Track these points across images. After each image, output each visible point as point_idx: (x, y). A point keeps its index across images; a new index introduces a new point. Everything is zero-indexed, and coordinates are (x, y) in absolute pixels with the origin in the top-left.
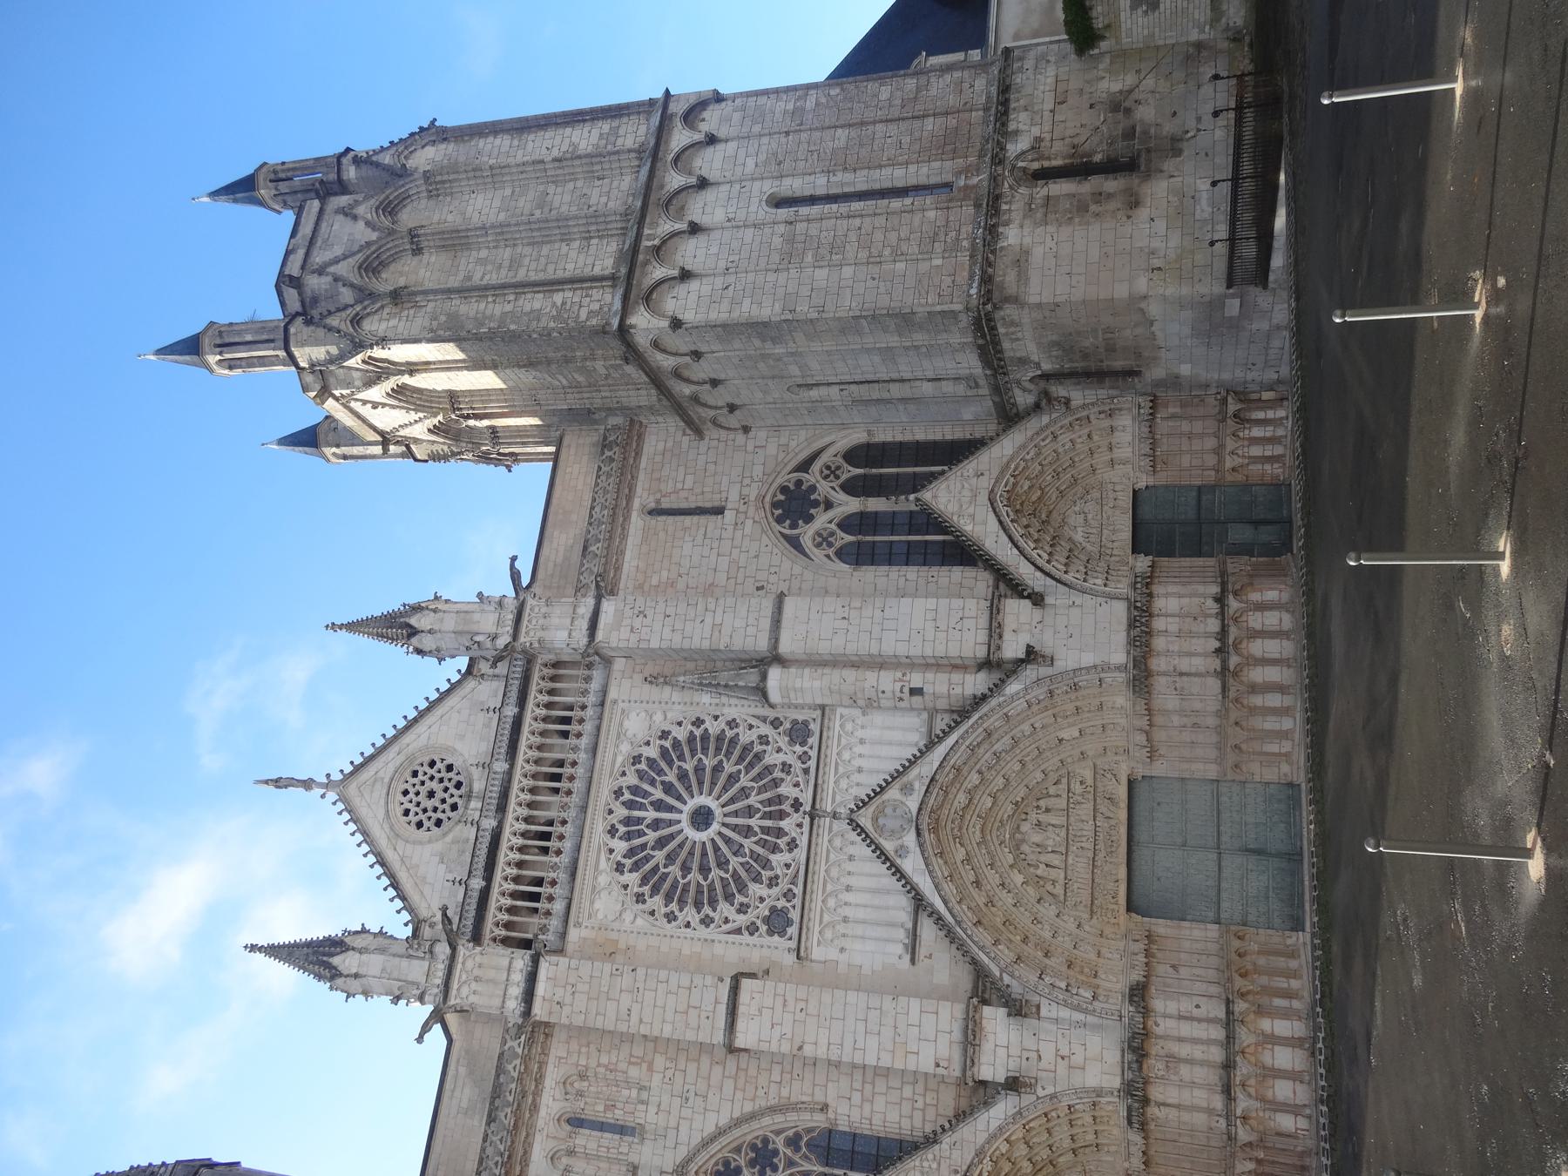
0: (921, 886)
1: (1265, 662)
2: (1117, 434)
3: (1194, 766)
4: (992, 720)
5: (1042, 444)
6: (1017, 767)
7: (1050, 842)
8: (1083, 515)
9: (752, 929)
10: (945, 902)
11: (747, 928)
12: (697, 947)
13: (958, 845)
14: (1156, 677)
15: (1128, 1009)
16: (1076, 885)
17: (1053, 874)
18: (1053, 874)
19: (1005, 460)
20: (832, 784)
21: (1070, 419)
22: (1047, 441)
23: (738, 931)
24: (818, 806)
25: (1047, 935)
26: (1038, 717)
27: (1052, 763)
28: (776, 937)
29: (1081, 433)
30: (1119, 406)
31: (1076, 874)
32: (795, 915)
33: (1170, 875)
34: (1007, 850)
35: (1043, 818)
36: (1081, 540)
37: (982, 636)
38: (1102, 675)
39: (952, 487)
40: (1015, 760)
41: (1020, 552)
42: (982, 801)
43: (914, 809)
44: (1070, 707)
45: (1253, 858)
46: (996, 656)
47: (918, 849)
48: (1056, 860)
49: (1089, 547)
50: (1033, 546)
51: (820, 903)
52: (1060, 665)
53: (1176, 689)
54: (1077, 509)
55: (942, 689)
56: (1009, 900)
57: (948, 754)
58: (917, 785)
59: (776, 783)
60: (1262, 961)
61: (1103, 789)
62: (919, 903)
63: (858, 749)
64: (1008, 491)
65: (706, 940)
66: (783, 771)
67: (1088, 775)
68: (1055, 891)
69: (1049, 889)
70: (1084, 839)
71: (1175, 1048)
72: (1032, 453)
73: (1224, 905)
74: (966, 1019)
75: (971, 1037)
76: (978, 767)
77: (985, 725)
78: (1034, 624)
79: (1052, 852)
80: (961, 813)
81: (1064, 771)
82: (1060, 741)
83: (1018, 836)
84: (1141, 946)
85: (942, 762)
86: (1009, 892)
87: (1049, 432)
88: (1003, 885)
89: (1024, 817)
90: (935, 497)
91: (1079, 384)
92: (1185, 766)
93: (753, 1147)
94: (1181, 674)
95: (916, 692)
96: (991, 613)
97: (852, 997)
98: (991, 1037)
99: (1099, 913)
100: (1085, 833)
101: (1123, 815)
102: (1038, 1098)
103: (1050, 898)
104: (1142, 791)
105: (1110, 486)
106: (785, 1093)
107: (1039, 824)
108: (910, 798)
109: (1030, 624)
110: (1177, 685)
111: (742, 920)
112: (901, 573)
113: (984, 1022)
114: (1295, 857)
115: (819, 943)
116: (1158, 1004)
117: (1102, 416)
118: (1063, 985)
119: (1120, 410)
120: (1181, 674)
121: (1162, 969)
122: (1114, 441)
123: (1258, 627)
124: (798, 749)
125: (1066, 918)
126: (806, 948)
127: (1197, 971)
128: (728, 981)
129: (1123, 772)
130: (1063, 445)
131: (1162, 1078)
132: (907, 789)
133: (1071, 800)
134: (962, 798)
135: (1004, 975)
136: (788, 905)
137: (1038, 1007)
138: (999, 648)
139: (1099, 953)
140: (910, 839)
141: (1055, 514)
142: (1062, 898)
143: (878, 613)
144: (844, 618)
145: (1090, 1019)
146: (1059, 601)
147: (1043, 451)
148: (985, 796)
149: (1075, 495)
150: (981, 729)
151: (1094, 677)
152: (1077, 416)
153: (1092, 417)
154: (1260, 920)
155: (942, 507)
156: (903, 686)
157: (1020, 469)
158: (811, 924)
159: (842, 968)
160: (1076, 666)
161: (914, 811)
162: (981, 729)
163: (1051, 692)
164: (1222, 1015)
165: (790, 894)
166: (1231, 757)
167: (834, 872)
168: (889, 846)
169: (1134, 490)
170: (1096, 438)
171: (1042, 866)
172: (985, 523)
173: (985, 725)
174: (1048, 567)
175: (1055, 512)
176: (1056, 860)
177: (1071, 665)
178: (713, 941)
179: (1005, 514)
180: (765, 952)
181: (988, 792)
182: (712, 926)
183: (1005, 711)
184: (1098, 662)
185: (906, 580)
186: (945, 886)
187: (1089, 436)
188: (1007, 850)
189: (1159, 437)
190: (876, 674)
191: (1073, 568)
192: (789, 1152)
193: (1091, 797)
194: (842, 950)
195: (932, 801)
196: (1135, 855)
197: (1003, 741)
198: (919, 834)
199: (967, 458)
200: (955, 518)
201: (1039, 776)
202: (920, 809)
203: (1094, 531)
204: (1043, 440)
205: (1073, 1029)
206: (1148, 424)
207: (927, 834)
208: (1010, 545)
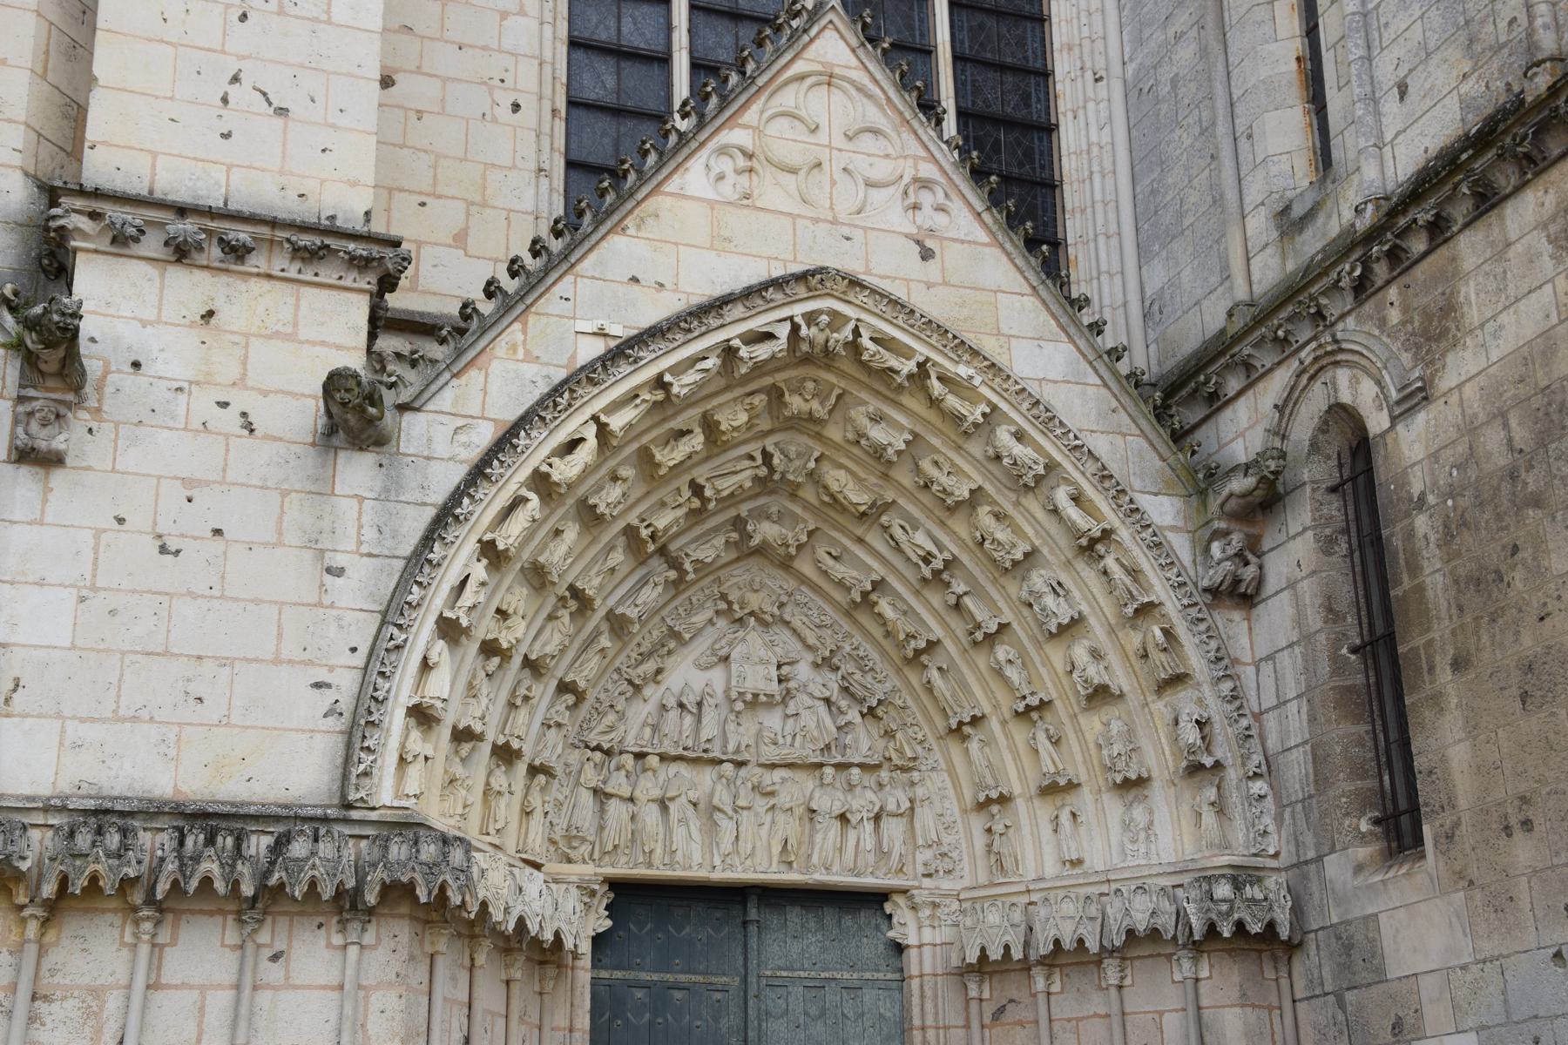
2: (1114, 807)
5: (1062, 496)
8: (774, 688)
21: (1172, 606)
22: (1072, 512)
29: (1113, 658)
30: (1234, 798)
39: (867, 142)
41: (589, 367)
46: (83, 223)
49: (641, 711)
50: (616, 422)
54: (803, 671)
64: (854, 346)
72: (1018, 450)
78: (240, 401)
87: (1112, 519)
90: (829, 79)
91: (1331, 612)
96: (304, 228)
105: (896, 798)
109: (240, 383)
117: (1191, 735)
119: (1220, 808)
122: (1085, 799)
130: (1057, 589)
138: (122, 240)
141: (779, 582)
146: (348, 508)
147: (1033, 504)
149: (861, 663)
152: (1181, 630)
153: (1185, 702)
155: (788, 98)
157: (952, 401)
169: (874, 900)
170: (1093, 724)
172: (720, 242)
174: (514, 478)
175: (791, 584)
179: (756, 324)
185: (504, 15)
187: (1100, 695)
189: (1112, 977)
191: (517, 597)
199: (995, 200)
203: (710, 728)
206: (1166, 922)
208: (619, 330)
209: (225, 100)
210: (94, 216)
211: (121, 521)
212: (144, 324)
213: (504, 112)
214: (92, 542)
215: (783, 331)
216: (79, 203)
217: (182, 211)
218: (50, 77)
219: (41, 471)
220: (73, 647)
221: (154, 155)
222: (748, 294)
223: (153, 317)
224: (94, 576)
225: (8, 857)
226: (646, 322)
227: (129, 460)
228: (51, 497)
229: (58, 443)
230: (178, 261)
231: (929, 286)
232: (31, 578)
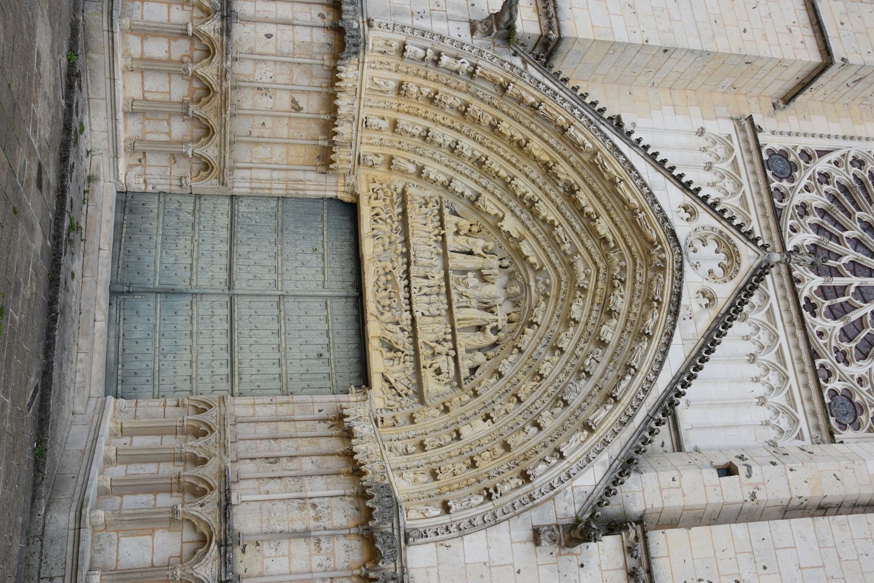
0: (651, 169)
3: (269, 411)
4: (612, 418)
6: (545, 369)
7: (472, 279)
9: (807, 156)
10: (614, 145)
11: (810, 158)
12: (859, 131)
13: (610, 238)
14: (353, 523)
16: (430, 227)
17: (462, 242)
18: (462, 242)
20: (781, 332)
23: (822, 153)
25: (467, 145)
26: (533, 442)
27: (489, 388)
28: (777, 147)
31: (431, 242)
33: (300, 257)
34: (532, 259)
35: (488, 316)
38: (446, 519)
40: (550, 379)
42: (586, 311)
43: (689, 273)
44: (484, 465)
45: (182, 286)
46: (632, 535)
47: (669, 216)
48: (458, 261)
51: (744, 181)
52: (521, 529)
53: (314, 506)
55: (689, 477)
56: (523, 185)
57: (665, 353)
58: (696, 308)
59: (846, 335)
61: (408, 364)
65: (852, 138)
66: (844, 353)
67: (431, 384)
68: (455, 219)
69: (464, 220)
70: (426, 290)
73: (224, 221)
76: (609, 351)
77: (620, 408)
79: (465, 272)
80: (616, 282)
81: (467, 386)
82: (487, 417)
83: (517, 289)
84: (344, 129)
85: (670, 340)
86: (522, 196)
88: (532, 202)
89: (514, 316)
92: (283, 410)
94: (305, 534)
95: (728, 470)
99: (395, 193)
100: (426, 299)
101: (373, 328)
103: (459, 207)
104: (345, 367)
107: (489, 309)
108: (699, 288)
110: (312, 513)
111: (822, 165)
113: (535, 17)
114: (119, 288)
115: (729, 137)
116: (322, 37)
118: (445, 59)
120: (305, 534)
121: (312, 104)
124: (835, 384)
125: (442, 178)
126: (743, 130)
127: (264, 102)
128: (837, 59)
133: (450, 345)
134: (620, 303)
137: (473, 31)
138: (630, 550)
139: (395, 125)
140: (683, 230)
142: (446, 211)
145: (407, 21)
148: (583, 320)
150: (625, 401)
151: (459, 515)
154: (176, 205)
158: (746, 157)
159: (696, 111)
161: (687, 267)
162: (625, 401)
163: (526, 477)
166: (210, 417)
168: (705, 219)
171: (478, 250)
173: (620, 408)
176: (458, 261)
178: (844, 138)
180: (785, 128)
181: (581, 326)
182: (850, 159)
183: (594, 437)
184: (456, 544)
190: (795, 493)
193: (424, 352)
194: (701, 132)
195: (668, 283)
196: (350, 279)
197: (581, 397)
198: (673, 233)
201: (506, 368)
202: (681, 269)
205: (427, 10)
207: (663, 237)
209: (700, 580)
210: (636, 538)
211: (519, 572)
212: (599, 566)
214: (508, 563)
216: (640, 532)
217: (649, 571)
218: (685, 512)
219: (532, 539)
220: (466, 564)
221: (668, 556)
223: (603, 568)
224: (495, 566)
225: (383, 558)
227: (544, 571)
228: (523, 544)
229: (544, 543)
230: (629, 574)
232: (490, 543)
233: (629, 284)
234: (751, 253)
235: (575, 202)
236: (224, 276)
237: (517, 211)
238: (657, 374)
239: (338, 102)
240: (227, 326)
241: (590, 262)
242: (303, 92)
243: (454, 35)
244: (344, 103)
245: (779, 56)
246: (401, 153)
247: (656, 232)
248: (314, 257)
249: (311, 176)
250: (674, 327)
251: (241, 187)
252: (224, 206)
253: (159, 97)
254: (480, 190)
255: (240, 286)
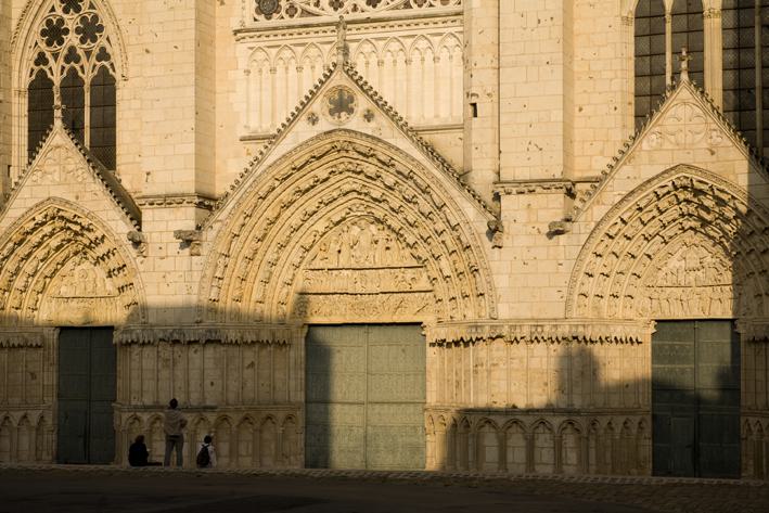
1: (503, 449)
4: (438, 192)
13: (330, 170)
15: (201, 329)
16: (324, 279)
19: (732, 177)
24: (349, 26)
32: (275, 21)
36: (671, 266)
37: (523, 174)
58: (373, 124)
60: (267, 435)
62: (273, 139)
63: (429, 56)
67: (424, 284)
71: (181, 366)
74: (183, 195)
75: (168, 201)
80: (358, 170)
84: (265, 336)
85: (393, 147)
93: (96, 17)
97: (190, 92)
98: (172, 217)
102: (135, 259)
106: (133, 40)
109: (537, 221)
110: (479, 368)
112: (619, 73)
116: (210, 351)
118: (218, 274)
123: (538, 443)
126: (244, 38)
127: (250, 384)
129: (428, 318)
131: (158, 357)
132: (369, 117)
135: (219, 224)
136: (283, 13)
143: (545, 58)
144: (539, 21)
150: (428, 182)
156: (477, 95)
160: (494, 270)
164: (208, 403)
165: (293, 11)
167: (287, 54)
172: (652, 162)
174: (600, 235)
177: (494, 266)
179: (662, 184)
185: (611, 80)
186: (287, 163)
188: (343, 215)
192: (96, 51)
194: (248, 72)
195: (358, 141)
196: (355, 330)
200: (657, 129)
203: (681, 277)
204: (759, 219)
208: (624, 193)
213: (612, 111)
215: (670, 184)
222: (657, 176)
226: (631, 189)
231: (713, 163)
233: (358, 162)
234: (338, 77)
235: (307, 190)
236: (355, 407)
237: (311, 223)
238: (413, 160)
239: (249, 341)
240: (386, 406)
241: (346, 181)
242: (243, 362)
243: (201, 268)
244: (250, 338)
245: (193, 22)
246: (276, 294)
247: (326, 144)
248: (344, 352)
249: (292, 353)
250: (385, 143)
251: (301, 397)
252: (312, 406)
253: (250, 446)
254: (298, 246)
255: (362, 399)
